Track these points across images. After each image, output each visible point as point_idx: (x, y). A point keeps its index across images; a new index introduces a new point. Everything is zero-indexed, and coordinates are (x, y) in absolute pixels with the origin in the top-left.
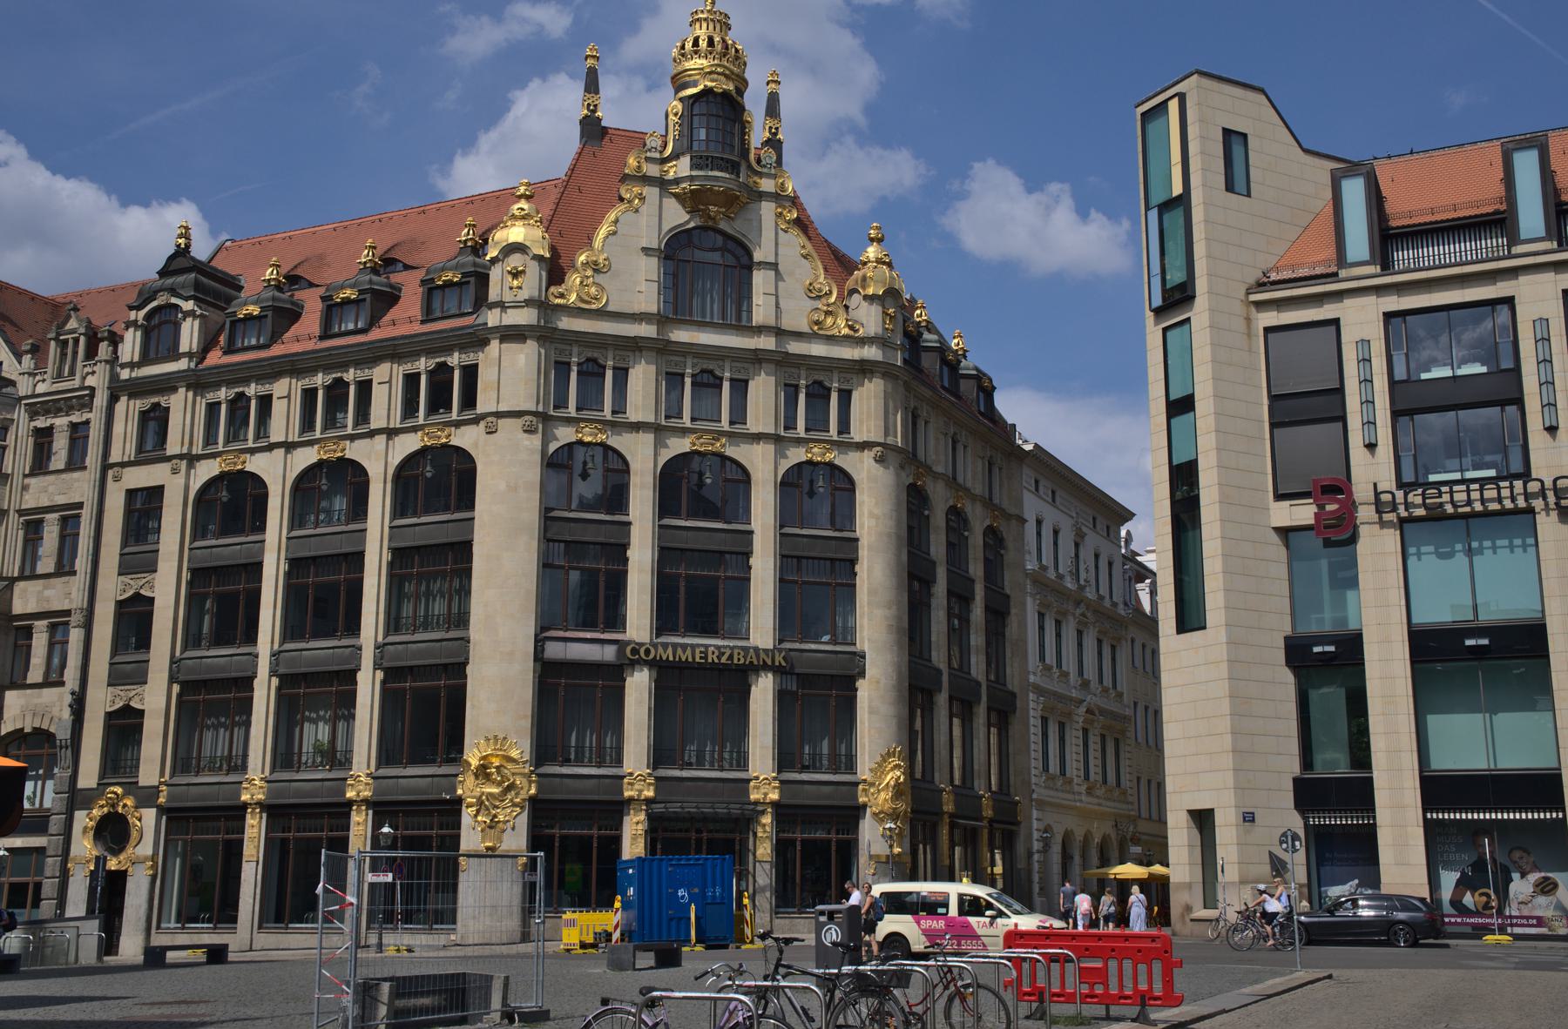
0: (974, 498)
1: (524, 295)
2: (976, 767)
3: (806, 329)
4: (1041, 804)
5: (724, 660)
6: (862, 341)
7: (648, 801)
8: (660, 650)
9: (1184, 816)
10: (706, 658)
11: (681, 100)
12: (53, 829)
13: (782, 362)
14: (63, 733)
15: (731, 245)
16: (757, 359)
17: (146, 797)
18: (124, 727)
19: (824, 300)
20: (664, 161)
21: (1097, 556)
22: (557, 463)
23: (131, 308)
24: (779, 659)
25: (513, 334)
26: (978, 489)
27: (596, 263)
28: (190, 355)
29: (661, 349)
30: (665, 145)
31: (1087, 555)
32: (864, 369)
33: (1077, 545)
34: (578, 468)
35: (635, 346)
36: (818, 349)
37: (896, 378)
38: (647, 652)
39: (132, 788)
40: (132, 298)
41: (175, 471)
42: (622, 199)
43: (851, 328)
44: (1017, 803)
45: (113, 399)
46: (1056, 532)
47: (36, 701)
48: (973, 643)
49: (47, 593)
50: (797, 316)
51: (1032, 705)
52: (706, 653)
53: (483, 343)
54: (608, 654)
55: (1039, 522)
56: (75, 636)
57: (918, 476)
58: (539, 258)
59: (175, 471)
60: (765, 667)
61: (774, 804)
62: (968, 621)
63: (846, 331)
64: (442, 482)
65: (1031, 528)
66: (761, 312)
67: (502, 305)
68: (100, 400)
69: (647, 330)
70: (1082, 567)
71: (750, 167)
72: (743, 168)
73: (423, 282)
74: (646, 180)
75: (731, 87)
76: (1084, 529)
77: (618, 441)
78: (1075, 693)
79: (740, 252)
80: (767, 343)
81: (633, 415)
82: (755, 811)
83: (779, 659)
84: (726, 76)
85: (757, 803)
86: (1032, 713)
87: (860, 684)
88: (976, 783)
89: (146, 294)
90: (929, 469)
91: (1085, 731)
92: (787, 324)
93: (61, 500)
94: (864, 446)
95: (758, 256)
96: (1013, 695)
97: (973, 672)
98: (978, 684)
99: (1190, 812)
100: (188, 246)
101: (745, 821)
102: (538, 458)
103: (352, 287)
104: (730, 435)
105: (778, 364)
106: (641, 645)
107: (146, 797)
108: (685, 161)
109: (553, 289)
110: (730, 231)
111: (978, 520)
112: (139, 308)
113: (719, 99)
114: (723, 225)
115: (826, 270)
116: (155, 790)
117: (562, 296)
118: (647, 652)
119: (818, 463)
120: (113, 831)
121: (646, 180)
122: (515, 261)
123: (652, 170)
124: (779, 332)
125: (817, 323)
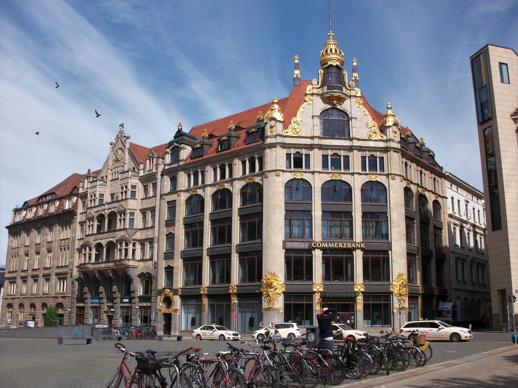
0: (429, 191)
1: (274, 133)
2: (432, 278)
4: (456, 290)
5: (344, 247)
6: (386, 141)
7: (321, 292)
9: (496, 292)
11: (323, 69)
12: (152, 301)
13: (360, 149)
14: (153, 273)
15: (342, 113)
16: (351, 149)
17: (176, 292)
18: (170, 271)
19: (373, 128)
20: (318, 88)
21: (474, 209)
22: (289, 186)
23: (166, 148)
25: (272, 146)
26: (431, 188)
27: (297, 121)
28: (183, 160)
29: (321, 147)
30: (318, 84)
31: (470, 208)
32: (386, 150)
33: (466, 205)
34: (295, 187)
35: (311, 147)
36: (371, 144)
37: (398, 152)
38: (319, 245)
39: (171, 289)
40: (167, 146)
41: (179, 196)
42: (305, 101)
43: (382, 137)
44: (447, 290)
45: (162, 175)
46: (459, 201)
47: (146, 264)
48: (430, 238)
49: (148, 233)
51: (452, 258)
53: (264, 149)
54: (306, 246)
55: (452, 198)
56: (156, 245)
57: (408, 184)
58: (280, 121)
59: (179, 196)
60: (358, 248)
61: (362, 293)
62: (428, 231)
64: (254, 194)
65: (449, 200)
66: (354, 133)
67: (268, 137)
68: (159, 176)
69: (316, 141)
70: (469, 213)
71: (346, 88)
72: (344, 88)
73: (246, 132)
74: (312, 94)
75: (338, 63)
76: (469, 200)
77: (307, 177)
78: (467, 254)
79: (344, 115)
81: (312, 170)
82: (356, 294)
83: (363, 246)
84: (337, 61)
85: (357, 292)
86: (452, 260)
87: (390, 252)
88: (432, 284)
89: (171, 144)
90: (412, 183)
91: (471, 266)
93: (150, 206)
95: (350, 117)
96: (445, 255)
97: (430, 248)
98: (432, 252)
99: (499, 290)
100: (181, 129)
101: (353, 299)
102: (281, 184)
103: (226, 136)
104: (344, 174)
106: (317, 243)
107: (176, 292)
108: (326, 88)
109: (285, 131)
110: (341, 108)
111: (431, 198)
112: (168, 148)
113: (335, 68)
114: (338, 107)
115: (373, 119)
116: (177, 290)
117: (287, 132)
118: (319, 245)
119: (373, 181)
120: (168, 301)
121: (312, 94)
122: (273, 123)
123: (315, 91)
124: (359, 140)
125: (370, 136)
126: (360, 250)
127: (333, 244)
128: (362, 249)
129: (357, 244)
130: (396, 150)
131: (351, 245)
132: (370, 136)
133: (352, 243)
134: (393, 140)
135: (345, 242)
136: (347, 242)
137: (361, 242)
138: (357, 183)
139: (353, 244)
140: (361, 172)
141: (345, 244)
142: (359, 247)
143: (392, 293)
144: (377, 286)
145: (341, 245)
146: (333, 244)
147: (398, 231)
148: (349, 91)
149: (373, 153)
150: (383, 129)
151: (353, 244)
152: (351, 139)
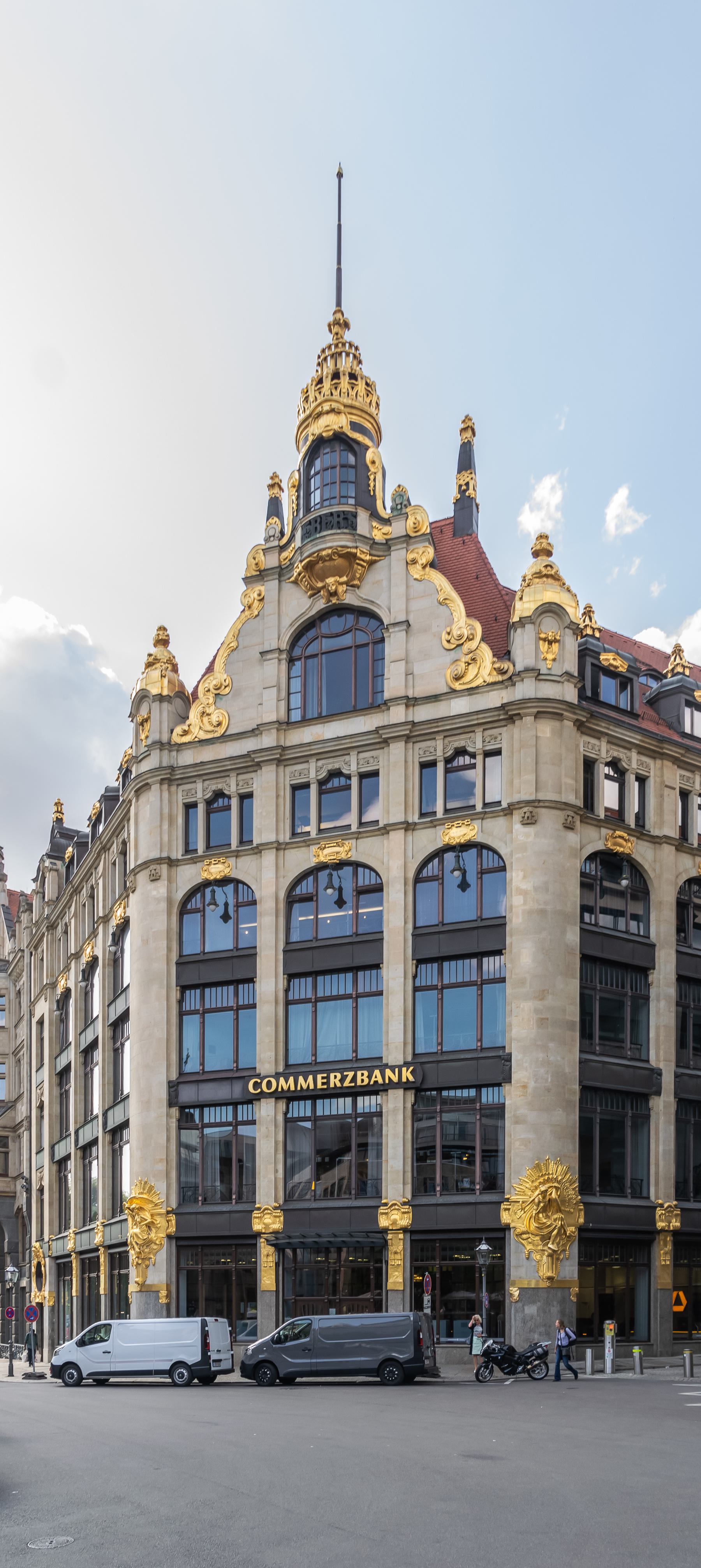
3: (445, 690)
5: (347, 1083)
8: (282, 1080)
10: (328, 1083)
16: (381, 739)
19: (465, 648)
24: (407, 1075)
36: (459, 706)
50: (433, 676)
52: (328, 1078)
61: (405, 1230)
63: (490, 680)
66: (393, 683)
80: (397, 714)
85: (385, 1231)
92: (419, 691)
94: (509, 811)
95: (386, 622)
105: (408, 738)
126: (400, 1092)
127: (310, 1078)
128: (406, 1086)
129: (388, 1072)
130: (547, 710)
131: (369, 1077)
132: (457, 678)
133: (383, 1068)
134: (537, 675)
135: (350, 1069)
136: (356, 1070)
137: (406, 1064)
138: (393, 859)
139: (377, 1072)
140: (414, 818)
141: (351, 1074)
142: (395, 1079)
143: (507, 1228)
144: (453, 1208)
145: (335, 1080)
146: (310, 1078)
147: (537, 1011)
148: (386, 529)
149: (459, 742)
150: (499, 639)
151: (377, 1072)
152: (384, 705)
